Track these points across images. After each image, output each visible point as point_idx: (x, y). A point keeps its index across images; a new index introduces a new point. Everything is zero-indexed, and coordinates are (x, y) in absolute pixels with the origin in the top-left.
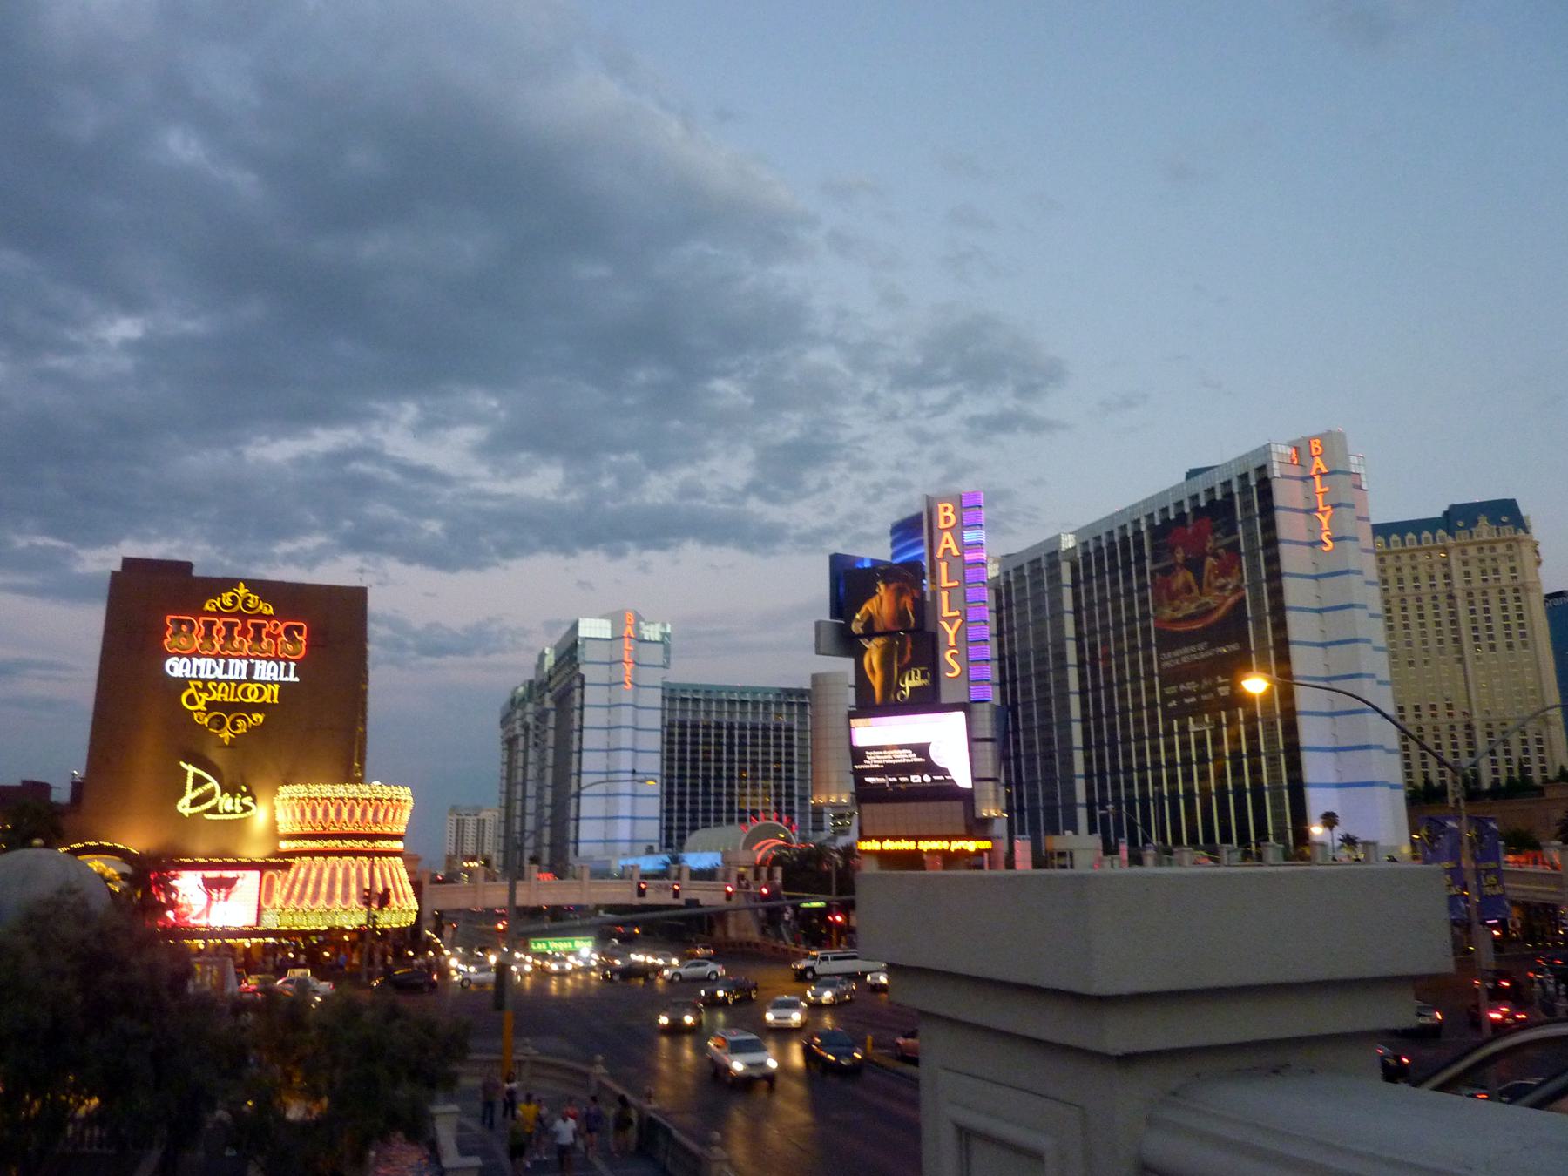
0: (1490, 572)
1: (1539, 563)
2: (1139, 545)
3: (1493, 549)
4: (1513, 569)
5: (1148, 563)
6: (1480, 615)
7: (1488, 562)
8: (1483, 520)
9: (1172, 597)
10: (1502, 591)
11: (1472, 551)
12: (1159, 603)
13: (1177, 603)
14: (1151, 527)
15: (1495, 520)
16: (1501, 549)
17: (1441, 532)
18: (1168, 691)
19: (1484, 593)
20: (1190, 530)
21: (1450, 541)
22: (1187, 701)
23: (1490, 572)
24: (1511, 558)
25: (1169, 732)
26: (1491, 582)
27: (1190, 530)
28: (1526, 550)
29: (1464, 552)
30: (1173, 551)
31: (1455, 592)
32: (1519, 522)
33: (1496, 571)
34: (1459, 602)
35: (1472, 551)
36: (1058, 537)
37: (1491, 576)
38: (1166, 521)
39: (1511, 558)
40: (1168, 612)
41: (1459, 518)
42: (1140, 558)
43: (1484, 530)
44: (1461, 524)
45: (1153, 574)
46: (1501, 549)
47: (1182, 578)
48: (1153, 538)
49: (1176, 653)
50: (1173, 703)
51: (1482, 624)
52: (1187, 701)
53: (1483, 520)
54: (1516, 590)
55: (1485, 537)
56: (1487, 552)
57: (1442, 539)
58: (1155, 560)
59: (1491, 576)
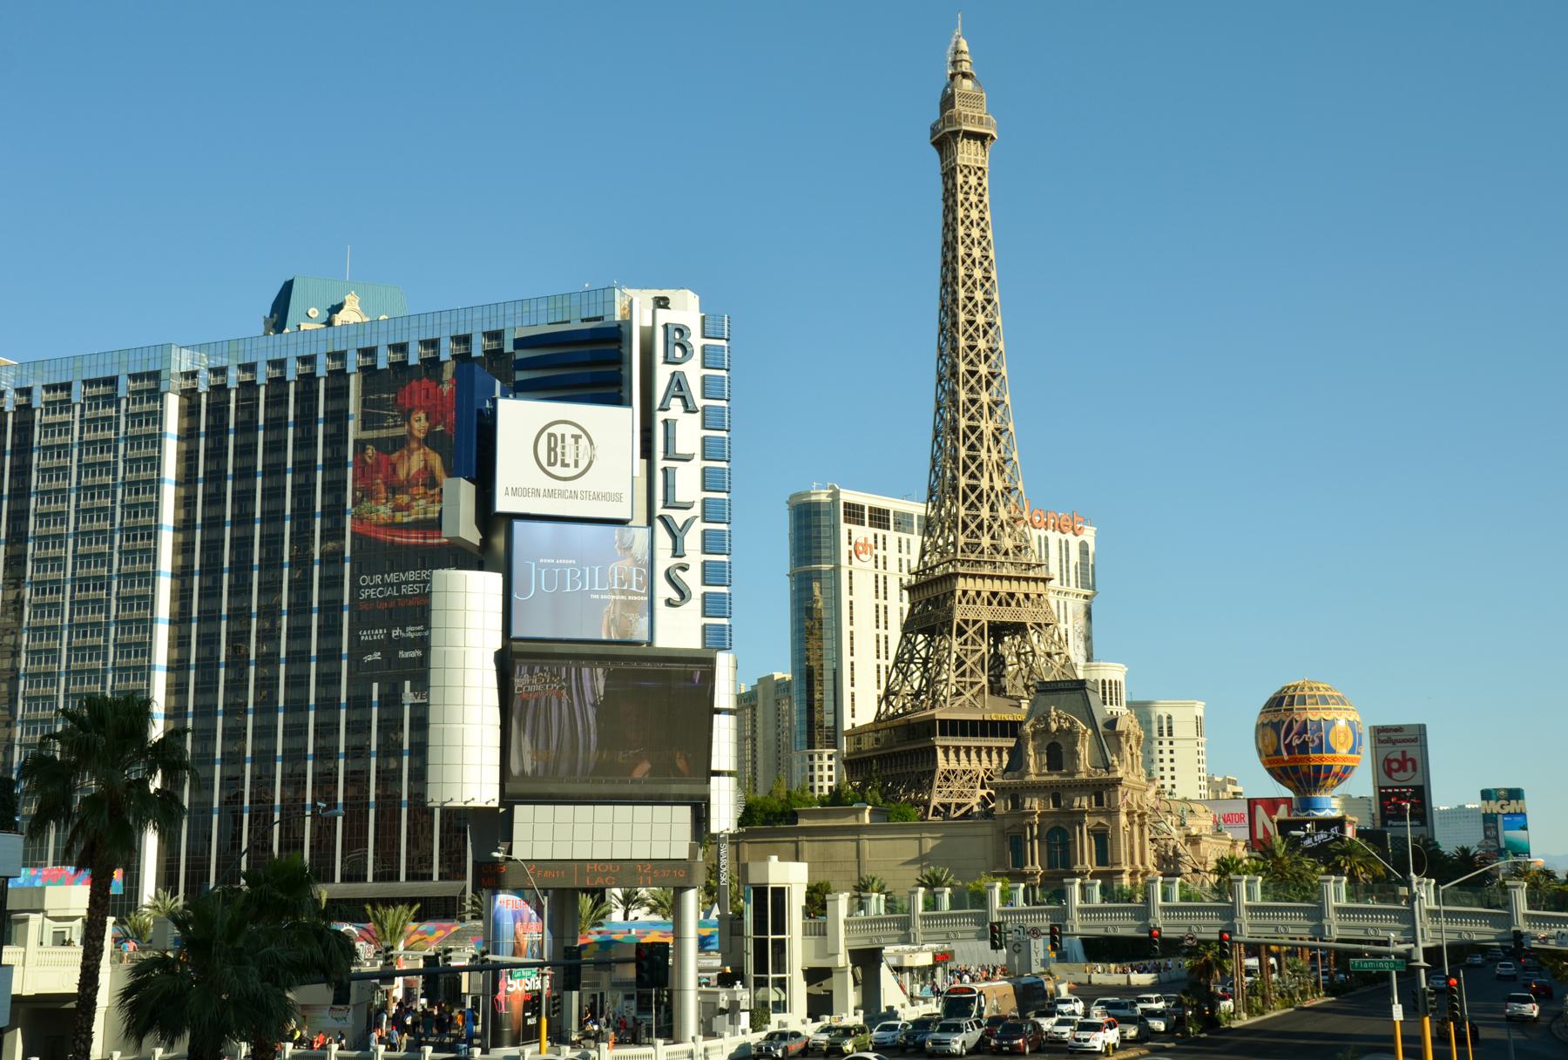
2: (338, 390)
5: (353, 430)
9: (394, 489)
12: (366, 494)
13: (404, 499)
14: (369, 372)
18: (365, 636)
20: (446, 388)
22: (402, 654)
25: (359, 702)
27: (446, 388)
30: (406, 416)
36: (164, 350)
38: (400, 367)
40: (384, 511)
42: (338, 418)
45: (360, 445)
47: (415, 462)
48: (366, 390)
49: (392, 577)
50: (377, 656)
52: (402, 654)
58: (367, 422)
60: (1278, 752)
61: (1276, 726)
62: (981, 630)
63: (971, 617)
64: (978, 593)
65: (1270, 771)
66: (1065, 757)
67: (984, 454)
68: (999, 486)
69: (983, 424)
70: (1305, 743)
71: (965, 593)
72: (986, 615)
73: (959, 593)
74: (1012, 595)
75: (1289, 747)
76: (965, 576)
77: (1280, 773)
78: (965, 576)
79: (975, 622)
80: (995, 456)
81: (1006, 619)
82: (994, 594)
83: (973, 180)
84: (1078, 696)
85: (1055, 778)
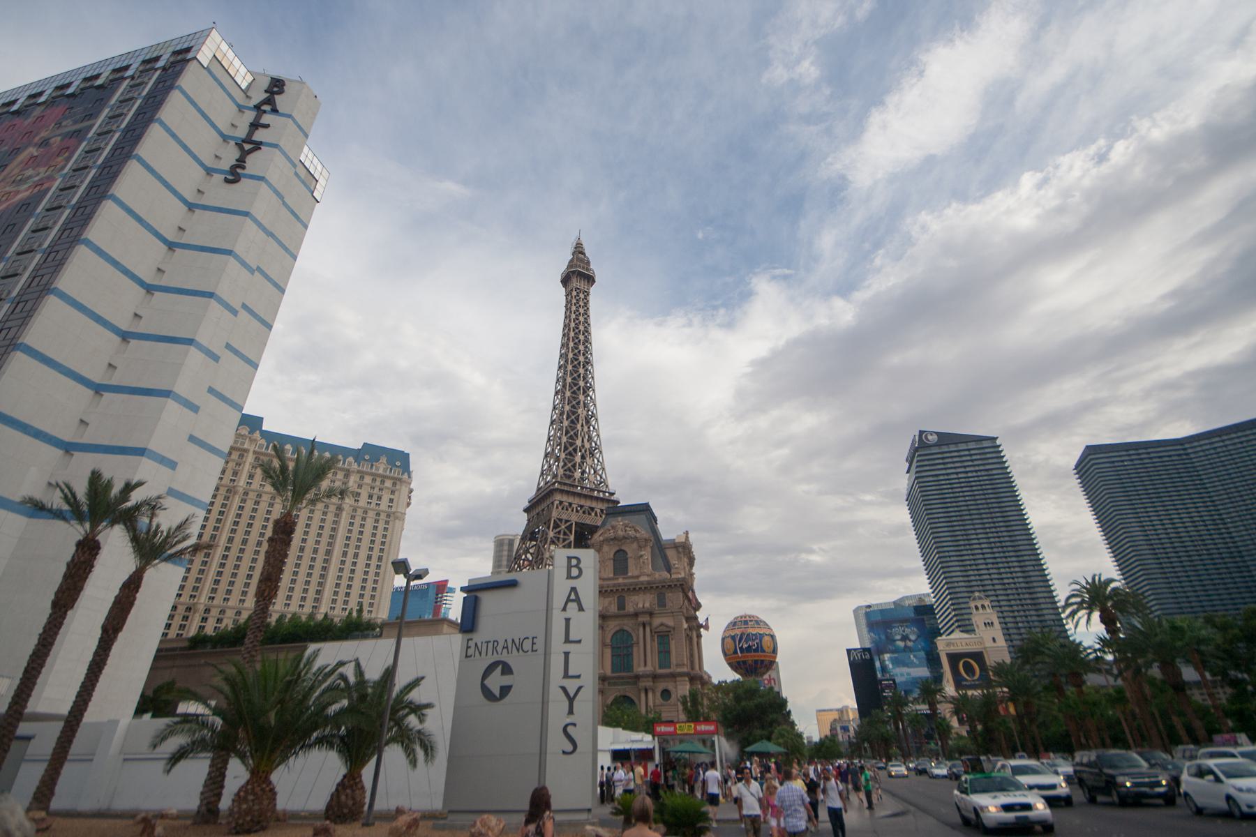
0: (375, 497)
1: (409, 504)
3: (383, 482)
4: (391, 500)
6: (346, 574)
7: (376, 490)
8: (384, 459)
10: (378, 514)
11: (368, 480)
15: (391, 462)
16: (388, 484)
17: (351, 459)
19: (365, 512)
21: (355, 466)
23: (375, 497)
24: (393, 492)
26: (373, 505)
28: (405, 490)
29: (362, 478)
31: (344, 506)
32: (406, 468)
33: (379, 498)
34: (344, 514)
35: (368, 480)
37: (374, 501)
39: (393, 492)
41: (370, 453)
43: (381, 467)
44: (367, 457)
46: (388, 484)
51: (355, 535)
53: (384, 459)
54: (388, 516)
55: (381, 471)
56: (378, 483)
57: (350, 464)
59: (374, 501)
60: (735, 652)
61: (733, 638)
62: (569, 528)
63: (564, 517)
64: (570, 504)
65: (730, 665)
66: (631, 563)
67: (579, 427)
68: (587, 445)
69: (580, 411)
70: (750, 647)
71: (561, 502)
72: (574, 518)
73: (556, 503)
74: (592, 509)
75: (741, 648)
76: (562, 491)
77: (735, 666)
78: (562, 491)
79: (567, 521)
80: (586, 429)
81: (588, 522)
82: (581, 507)
83: (582, 296)
84: (642, 517)
85: (621, 581)
